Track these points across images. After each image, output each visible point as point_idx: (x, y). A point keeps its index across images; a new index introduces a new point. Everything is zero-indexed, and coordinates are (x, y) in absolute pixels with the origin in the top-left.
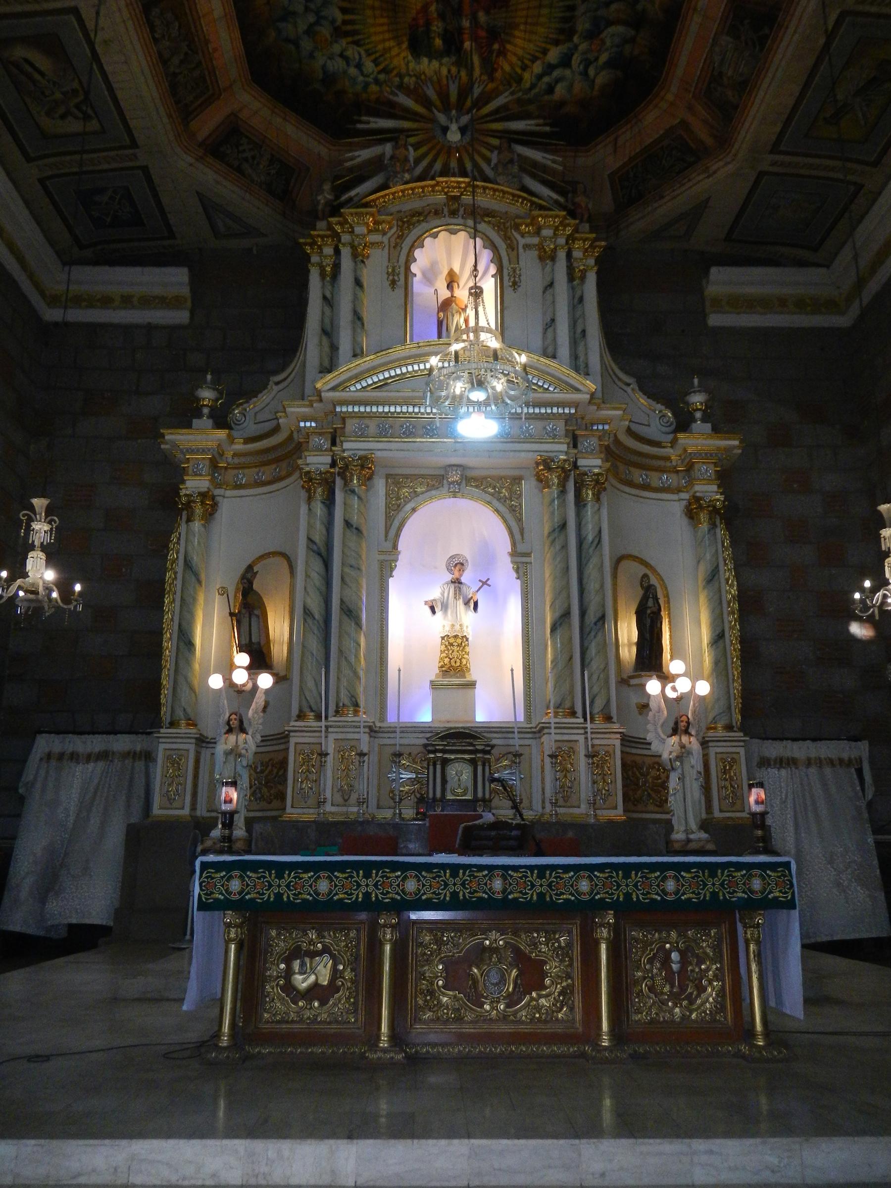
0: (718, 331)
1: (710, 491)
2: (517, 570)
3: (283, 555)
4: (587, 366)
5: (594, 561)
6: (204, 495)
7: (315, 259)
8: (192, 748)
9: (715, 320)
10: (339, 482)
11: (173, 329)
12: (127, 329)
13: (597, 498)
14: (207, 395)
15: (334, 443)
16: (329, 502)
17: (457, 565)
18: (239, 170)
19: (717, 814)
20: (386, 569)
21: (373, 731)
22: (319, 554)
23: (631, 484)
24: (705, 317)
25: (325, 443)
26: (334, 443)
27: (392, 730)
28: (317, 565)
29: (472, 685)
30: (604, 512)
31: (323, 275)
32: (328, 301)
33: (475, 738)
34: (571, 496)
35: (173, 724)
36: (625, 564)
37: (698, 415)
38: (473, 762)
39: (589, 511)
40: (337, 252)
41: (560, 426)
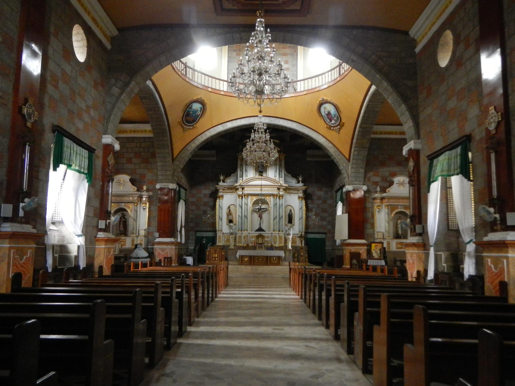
1: (301, 195)
5: (281, 208)
7: (239, 157)
9: (308, 159)
10: (243, 196)
13: (282, 198)
14: (222, 178)
15: (243, 190)
23: (289, 193)
26: (243, 190)
28: (240, 208)
30: (283, 200)
31: (240, 160)
34: (278, 199)
35: (219, 231)
37: (301, 182)
39: (281, 200)
41: (276, 189)
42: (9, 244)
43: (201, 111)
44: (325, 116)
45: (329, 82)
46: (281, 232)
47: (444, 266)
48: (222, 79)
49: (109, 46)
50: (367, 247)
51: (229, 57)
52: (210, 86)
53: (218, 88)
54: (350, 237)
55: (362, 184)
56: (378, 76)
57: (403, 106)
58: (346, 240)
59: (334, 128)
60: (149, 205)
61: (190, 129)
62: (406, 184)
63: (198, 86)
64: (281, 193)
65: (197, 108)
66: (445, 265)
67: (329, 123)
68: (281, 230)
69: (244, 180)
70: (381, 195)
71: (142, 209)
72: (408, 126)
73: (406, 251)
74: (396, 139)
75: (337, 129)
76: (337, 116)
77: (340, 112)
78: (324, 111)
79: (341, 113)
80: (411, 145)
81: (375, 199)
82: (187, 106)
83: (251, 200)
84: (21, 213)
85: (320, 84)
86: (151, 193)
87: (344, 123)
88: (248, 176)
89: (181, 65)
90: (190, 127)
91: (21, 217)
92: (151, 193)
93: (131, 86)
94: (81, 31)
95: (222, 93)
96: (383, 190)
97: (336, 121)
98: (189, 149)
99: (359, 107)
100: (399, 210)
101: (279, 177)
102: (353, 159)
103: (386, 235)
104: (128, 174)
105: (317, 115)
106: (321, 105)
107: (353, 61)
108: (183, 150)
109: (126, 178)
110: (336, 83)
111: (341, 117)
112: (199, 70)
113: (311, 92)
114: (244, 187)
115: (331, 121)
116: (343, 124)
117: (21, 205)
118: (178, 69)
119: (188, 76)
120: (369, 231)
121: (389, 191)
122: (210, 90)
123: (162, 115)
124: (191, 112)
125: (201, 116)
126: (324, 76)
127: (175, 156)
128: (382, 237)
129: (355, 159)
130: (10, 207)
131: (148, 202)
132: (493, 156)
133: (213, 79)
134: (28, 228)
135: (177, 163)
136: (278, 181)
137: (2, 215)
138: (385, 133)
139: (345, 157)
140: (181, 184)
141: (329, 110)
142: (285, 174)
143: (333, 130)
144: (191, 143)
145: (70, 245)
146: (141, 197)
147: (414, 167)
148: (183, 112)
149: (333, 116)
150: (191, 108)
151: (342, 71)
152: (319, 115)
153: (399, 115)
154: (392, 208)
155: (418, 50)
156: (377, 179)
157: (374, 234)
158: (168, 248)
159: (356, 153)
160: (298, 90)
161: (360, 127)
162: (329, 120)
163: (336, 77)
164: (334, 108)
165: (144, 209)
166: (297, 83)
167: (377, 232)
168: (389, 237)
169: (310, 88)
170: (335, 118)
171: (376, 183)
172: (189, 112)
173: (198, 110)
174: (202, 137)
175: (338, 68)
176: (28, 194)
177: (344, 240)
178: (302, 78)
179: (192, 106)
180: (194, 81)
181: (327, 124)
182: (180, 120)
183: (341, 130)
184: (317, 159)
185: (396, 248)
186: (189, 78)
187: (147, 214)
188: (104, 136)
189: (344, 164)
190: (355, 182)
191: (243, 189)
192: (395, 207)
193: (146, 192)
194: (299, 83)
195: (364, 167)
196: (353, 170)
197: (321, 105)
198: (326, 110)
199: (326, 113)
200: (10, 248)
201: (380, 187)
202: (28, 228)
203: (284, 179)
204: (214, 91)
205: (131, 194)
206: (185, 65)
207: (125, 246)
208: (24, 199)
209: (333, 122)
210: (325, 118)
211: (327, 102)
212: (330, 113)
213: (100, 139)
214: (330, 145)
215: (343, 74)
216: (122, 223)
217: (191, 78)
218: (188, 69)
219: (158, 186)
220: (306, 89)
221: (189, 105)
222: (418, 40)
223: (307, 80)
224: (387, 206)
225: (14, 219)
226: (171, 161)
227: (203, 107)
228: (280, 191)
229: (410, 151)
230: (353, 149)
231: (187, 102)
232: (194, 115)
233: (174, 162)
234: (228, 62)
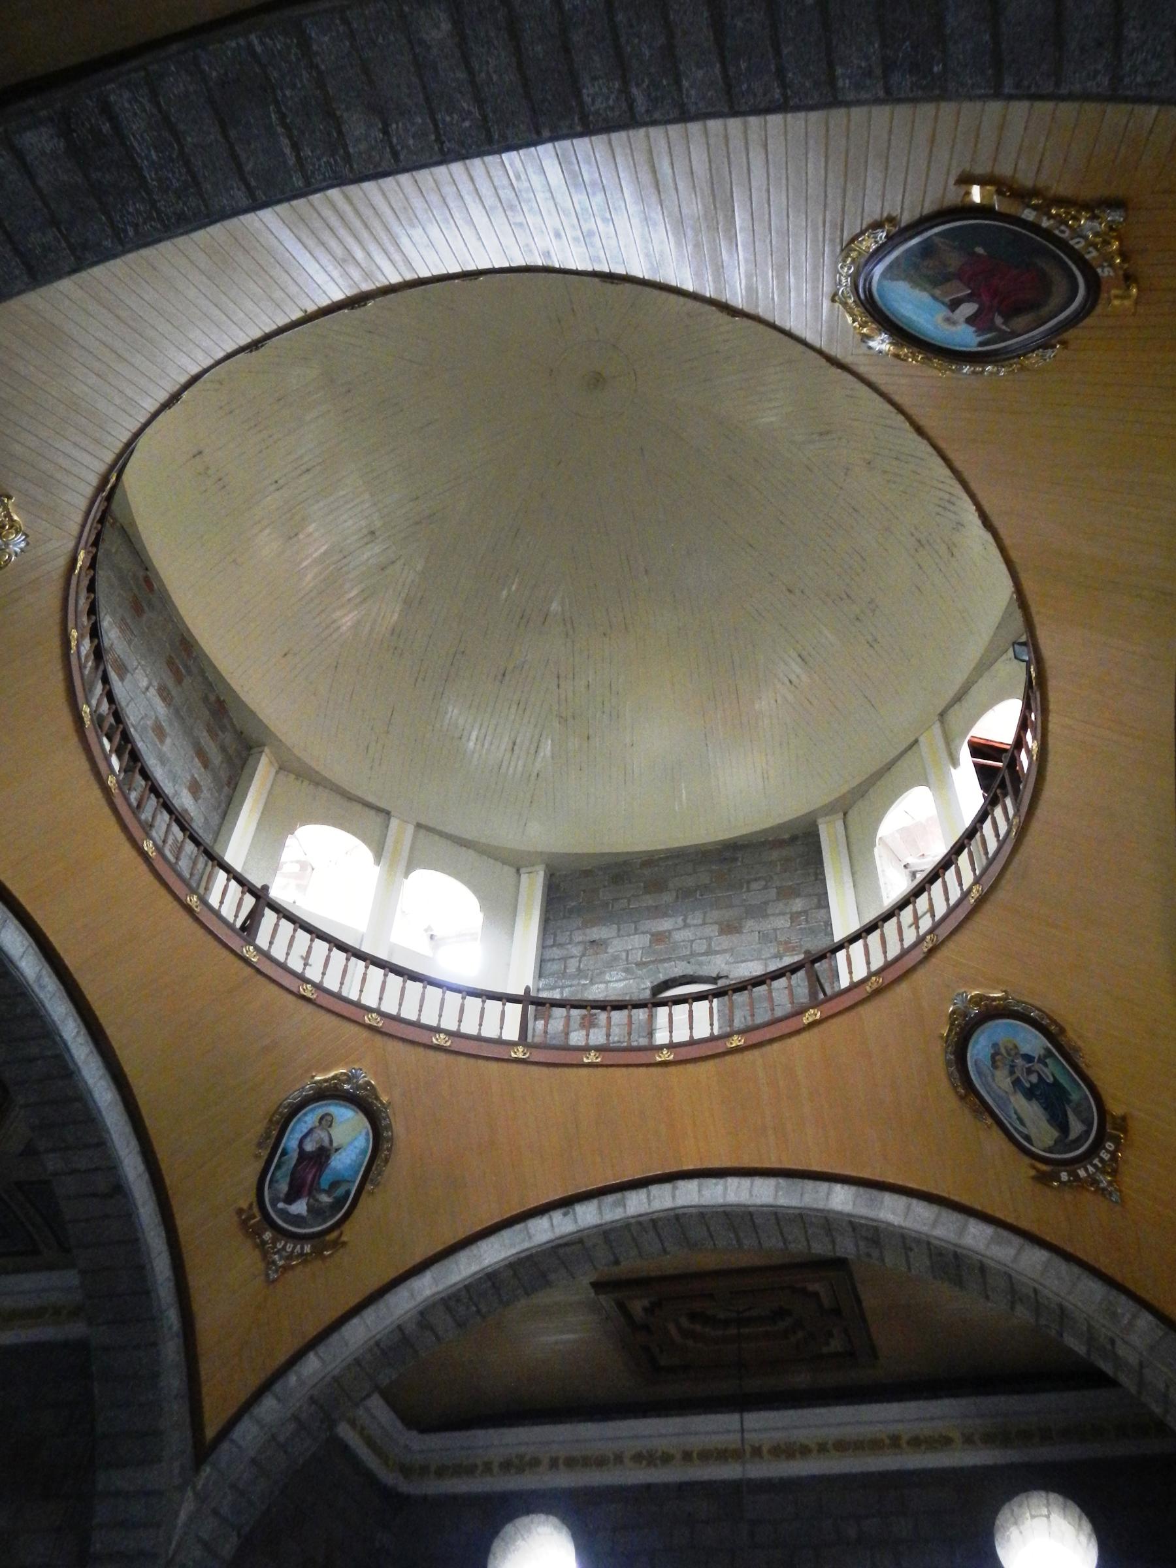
44: (294, 1156)
59: (274, 1241)
76: (348, 1193)
78: (310, 1132)
79: (372, 1193)
87: (344, 1244)
97: (316, 1212)
105: (260, 1128)
111: (356, 1212)
115: (291, 1198)
116: (337, 1244)
141: (335, 1144)
149: (325, 1182)
162: (291, 1185)
164: (364, 1152)
170: (325, 1199)
199: (309, 1147)
209: (300, 1207)
210: (278, 1167)
212: (328, 1157)
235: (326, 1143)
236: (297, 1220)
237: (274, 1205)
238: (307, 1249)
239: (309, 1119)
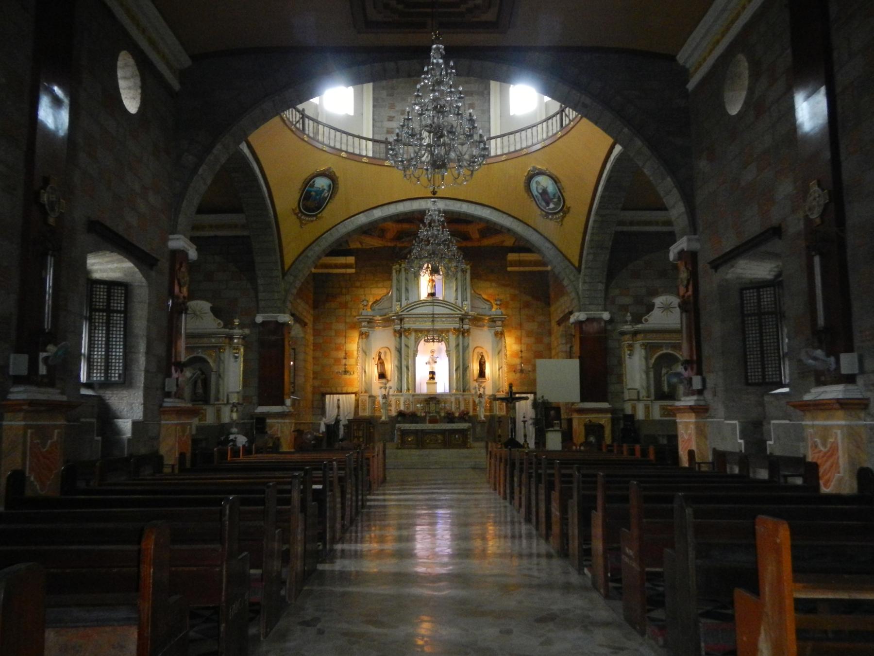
0: (510, 272)
2: (447, 355)
3: (387, 348)
4: (466, 298)
5: (467, 352)
6: (366, 332)
8: (367, 398)
9: (509, 269)
11: (350, 274)
12: (337, 275)
13: (468, 335)
15: (401, 323)
16: (400, 337)
17: (432, 352)
18: (371, 235)
19: (498, 413)
20: (415, 355)
21: (413, 396)
22: (398, 351)
23: (478, 326)
24: (506, 267)
25: (399, 322)
26: (401, 323)
27: (419, 395)
28: (397, 353)
29: (436, 383)
30: (470, 338)
32: (398, 281)
33: (436, 398)
34: (461, 336)
36: (476, 351)
38: (436, 404)
39: (466, 338)
40: (400, 265)
41: (457, 319)
42: (24, 419)
43: (329, 191)
44: (539, 195)
45: (544, 140)
46: (466, 393)
47: (740, 444)
48: (365, 135)
49: (176, 86)
50: (612, 414)
51: (375, 100)
52: (344, 148)
53: (357, 152)
54: (583, 399)
55: (600, 308)
56: (626, 130)
57: (669, 179)
58: (577, 403)
59: (553, 216)
60: (245, 351)
61: (312, 221)
62: (675, 308)
63: (324, 149)
64: (466, 327)
65: (323, 187)
66: (741, 441)
67: (545, 208)
68: (467, 387)
69: (403, 306)
70: (633, 327)
71: (232, 360)
72: (677, 211)
73: (678, 420)
74: (657, 233)
75: (559, 218)
77: (563, 189)
78: (537, 188)
79: (564, 192)
80: (682, 244)
81: (623, 333)
82: (305, 182)
83: (415, 338)
84: (43, 370)
85: (530, 143)
86: (247, 331)
87: (569, 207)
88: (410, 298)
89: (296, 115)
90: (312, 219)
91: (43, 376)
92: (247, 331)
93: (215, 151)
94: (131, 61)
95: (365, 160)
96: (637, 319)
97: (555, 204)
98: (309, 255)
99: (594, 180)
100: (665, 351)
101: (463, 301)
102: (586, 268)
103: (643, 393)
104: (207, 300)
105: (526, 195)
106: (530, 178)
107: (585, 106)
108: (301, 258)
109: (203, 306)
110: (554, 140)
112: (324, 122)
113: (514, 155)
114: (404, 318)
115: (548, 204)
116: (569, 208)
117: (43, 355)
118: (290, 122)
119: (307, 132)
120: (613, 388)
121: (646, 320)
122: (343, 154)
123: (263, 198)
124: (313, 193)
125: (330, 198)
126: (535, 129)
127: (286, 268)
128: (636, 398)
129: (589, 267)
130: (24, 359)
131: (242, 345)
132: (817, 260)
133: (349, 137)
134: (53, 395)
135: (290, 278)
136: (461, 306)
137: (11, 373)
138: (639, 223)
139: (574, 266)
140: (297, 314)
141: (545, 186)
142: (471, 294)
143: (551, 219)
144: (314, 245)
145: (120, 420)
146: (231, 338)
147: (688, 281)
148: (299, 192)
150: (312, 186)
151: (566, 121)
152: (529, 195)
153: (662, 194)
154: (650, 348)
155: (691, 86)
156: (627, 300)
157: (623, 393)
158: (278, 423)
159: (591, 257)
160: (493, 154)
161: (597, 213)
163: (555, 131)
165: (236, 358)
166: (490, 142)
167: (629, 389)
168: (648, 397)
169: (512, 149)
170: (555, 200)
171: (624, 308)
172: (309, 192)
173: (325, 189)
174: (331, 234)
175: (558, 116)
176: (53, 337)
177: (573, 404)
178: (499, 134)
179: (314, 182)
180: (318, 141)
181: (542, 210)
182: (294, 205)
183: (565, 219)
184: (527, 269)
185: (661, 417)
186: (308, 136)
187: (242, 365)
188: (171, 237)
189: (571, 277)
190: (590, 307)
191: (401, 320)
192: (659, 346)
193: (239, 329)
194: (493, 142)
195: (604, 281)
196: (586, 286)
197: (530, 178)
198: (540, 187)
199: (540, 191)
200: (27, 427)
201: (632, 314)
202: (53, 395)
203: (470, 303)
204: (351, 157)
205: (214, 334)
206: (302, 114)
207: (205, 421)
208: (46, 346)
209: (552, 206)
211: (541, 173)
213: (165, 241)
214: (547, 245)
215: (567, 126)
216: (199, 382)
217: (311, 135)
218: (307, 120)
219: (259, 319)
220: (506, 151)
221: (308, 182)
222: (691, 71)
223: (507, 137)
224: (643, 344)
225: (30, 379)
226: (281, 277)
227: (333, 184)
228: (464, 321)
229: (681, 253)
230: (585, 252)
231: (306, 175)
232: (318, 197)
233: (286, 278)
234: (374, 106)
235: (543, 188)
236: (553, 209)
237: (545, 208)
238: (562, 214)
239: (533, 185)
